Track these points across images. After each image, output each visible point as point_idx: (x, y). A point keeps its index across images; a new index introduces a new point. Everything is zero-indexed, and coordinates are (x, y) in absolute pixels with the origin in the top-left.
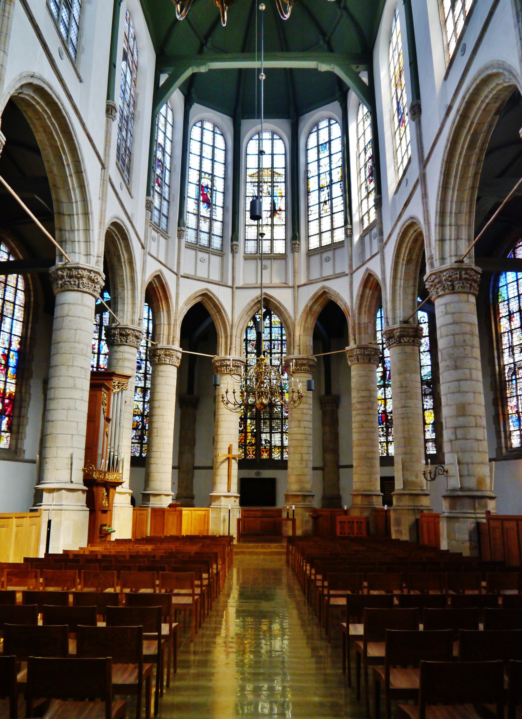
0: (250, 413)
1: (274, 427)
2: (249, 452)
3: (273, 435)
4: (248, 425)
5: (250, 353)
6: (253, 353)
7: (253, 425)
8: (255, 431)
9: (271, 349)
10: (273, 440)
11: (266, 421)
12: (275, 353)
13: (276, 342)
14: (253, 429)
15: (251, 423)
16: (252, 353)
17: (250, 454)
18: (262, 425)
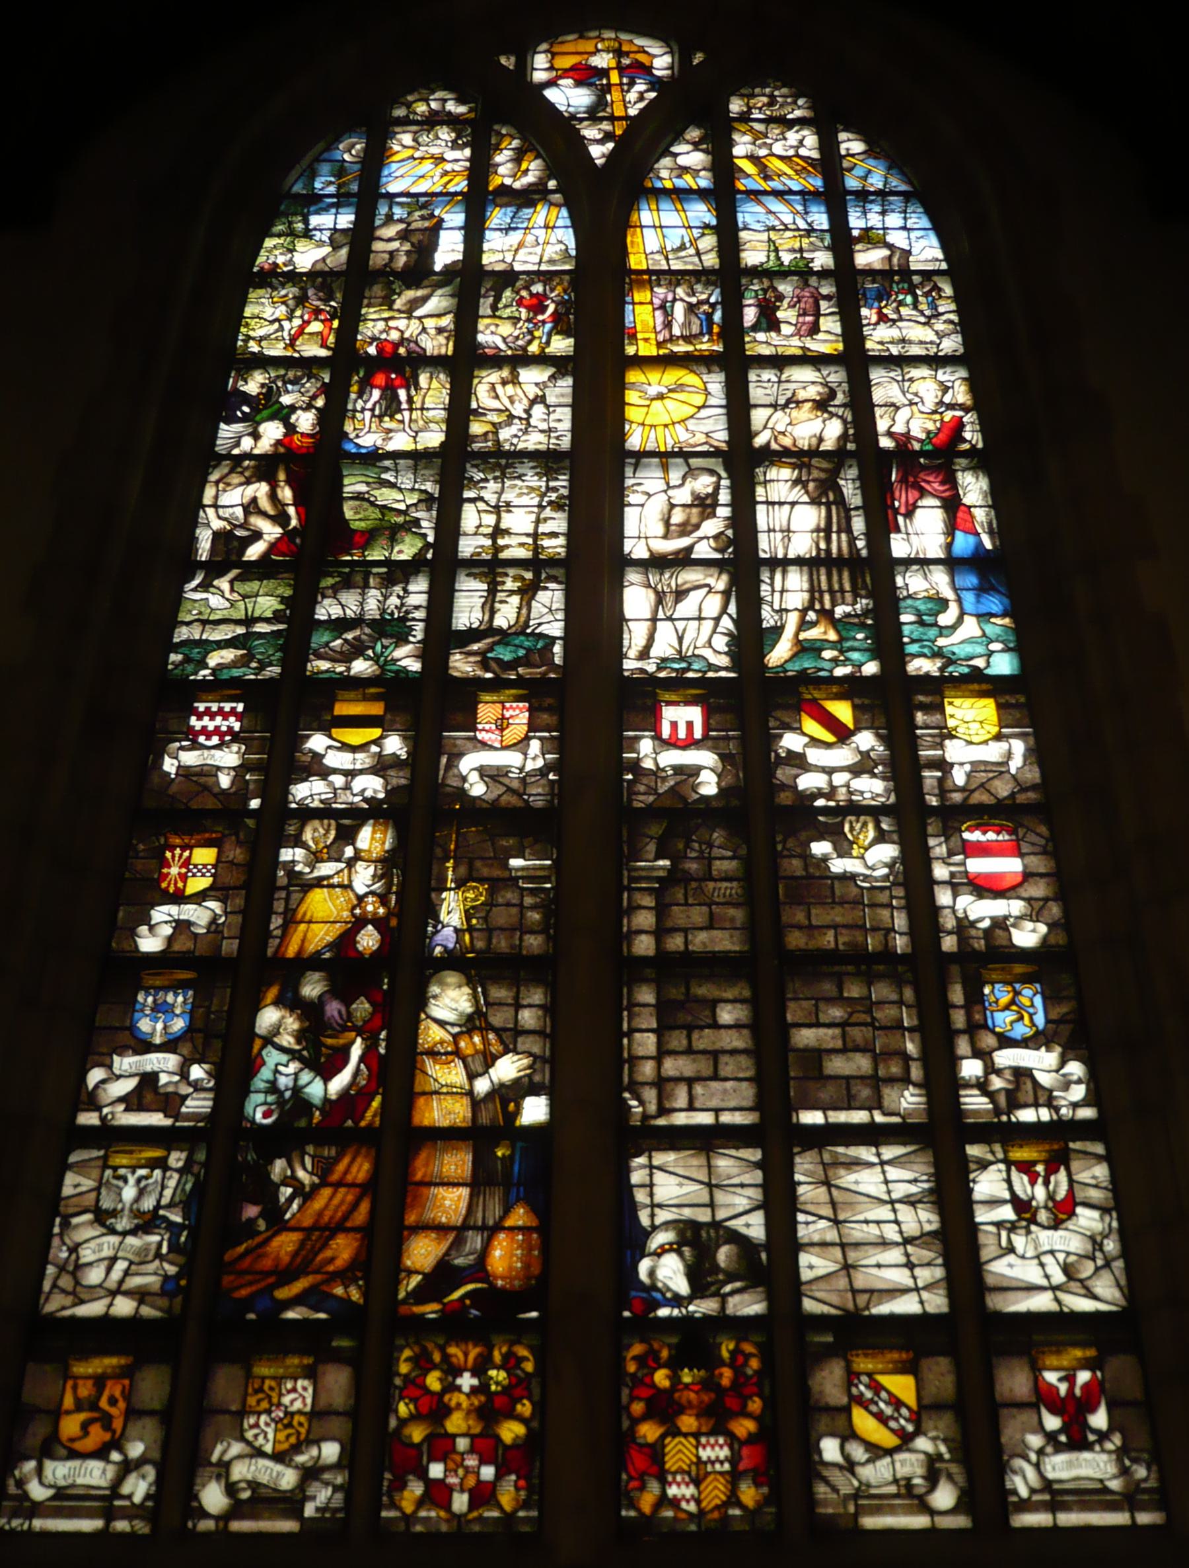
0: (476, 894)
1: (816, 1055)
2: (436, 1410)
3: (804, 1167)
4: (432, 1035)
5: (496, 361)
6: (542, 359)
7: (510, 1039)
8: (535, 1110)
9: (733, 331)
10: (810, 1229)
11: (703, 990)
12: (779, 362)
13: (785, 288)
14: (510, 1094)
15: (473, 1023)
16: (519, 360)
17: (441, 1446)
18: (647, 1043)
